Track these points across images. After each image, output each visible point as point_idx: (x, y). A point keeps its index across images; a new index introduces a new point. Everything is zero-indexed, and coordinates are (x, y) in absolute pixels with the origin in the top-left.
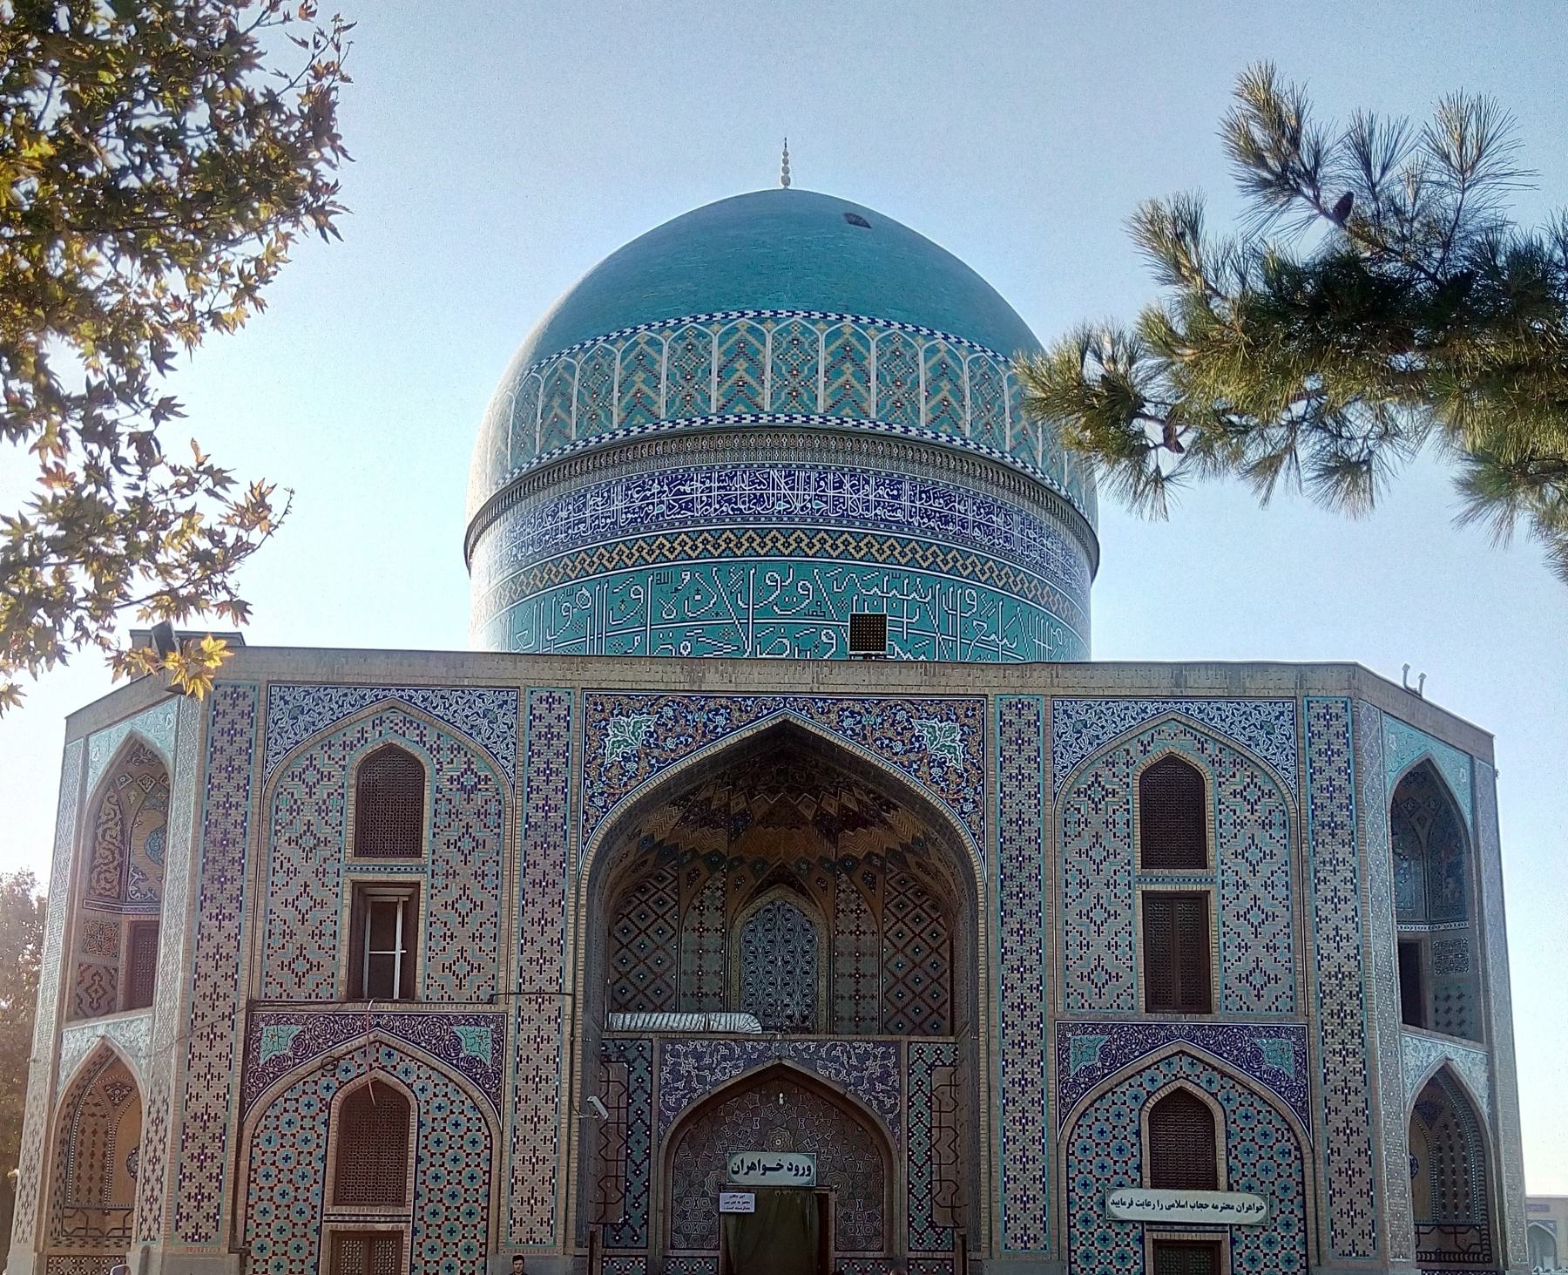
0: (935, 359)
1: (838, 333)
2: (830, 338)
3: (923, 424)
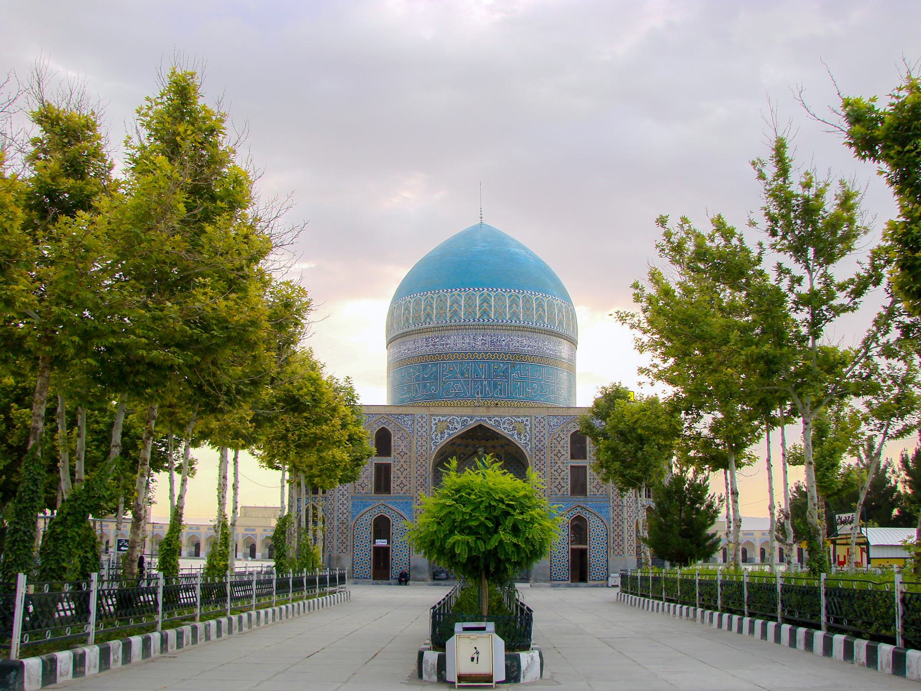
1: (483, 294)
2: (480, 296)
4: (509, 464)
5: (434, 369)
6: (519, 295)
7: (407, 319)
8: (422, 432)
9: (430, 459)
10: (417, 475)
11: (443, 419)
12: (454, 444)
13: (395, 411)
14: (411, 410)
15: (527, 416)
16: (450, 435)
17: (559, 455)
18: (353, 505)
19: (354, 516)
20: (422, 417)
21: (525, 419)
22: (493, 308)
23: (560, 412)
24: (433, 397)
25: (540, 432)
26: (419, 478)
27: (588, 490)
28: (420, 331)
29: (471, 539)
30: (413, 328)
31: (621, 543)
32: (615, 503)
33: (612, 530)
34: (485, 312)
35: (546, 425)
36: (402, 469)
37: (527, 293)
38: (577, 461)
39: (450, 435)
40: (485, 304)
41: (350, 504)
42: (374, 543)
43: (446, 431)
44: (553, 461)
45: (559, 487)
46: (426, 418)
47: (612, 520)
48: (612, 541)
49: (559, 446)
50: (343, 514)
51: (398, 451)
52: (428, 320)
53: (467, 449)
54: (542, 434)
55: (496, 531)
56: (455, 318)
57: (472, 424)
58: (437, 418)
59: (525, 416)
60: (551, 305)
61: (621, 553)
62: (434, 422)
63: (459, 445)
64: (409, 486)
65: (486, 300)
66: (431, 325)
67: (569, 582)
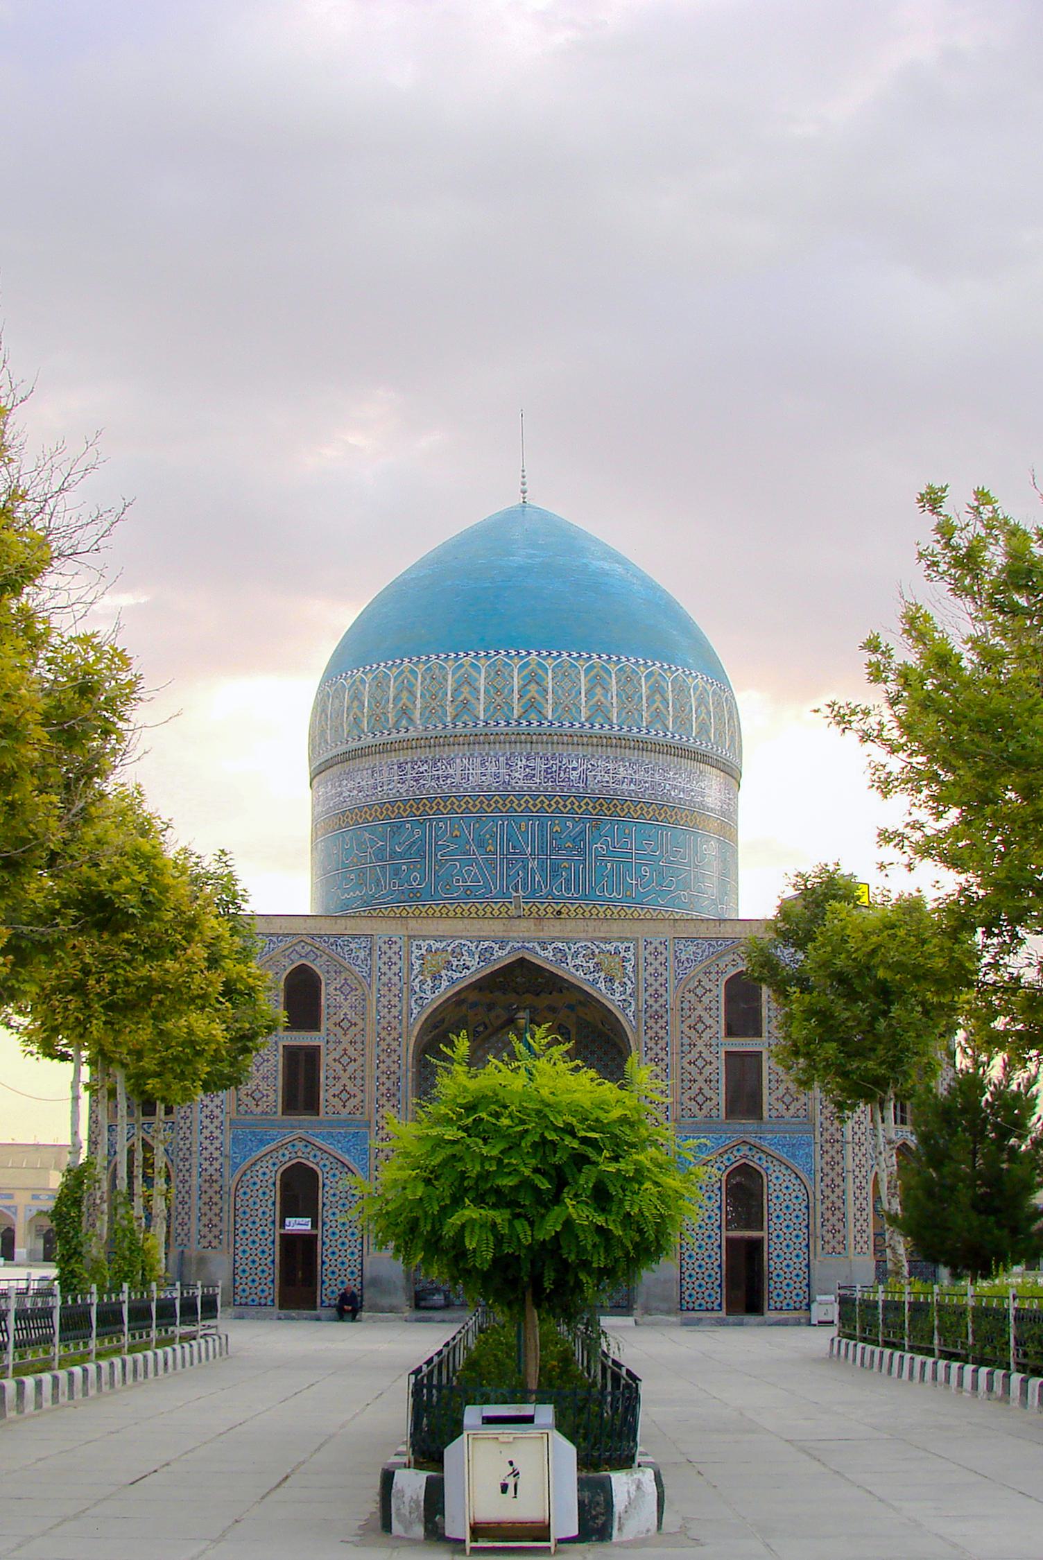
0: (592, 674)
1: (527, 665)
3: (583, 719)
4: (586, 1047)
5: (418, 833)
6: (610, 667)
7: (357, 721)
8: (390, 974)
9: (409, 1033)
10: (378, 1073)
12: (463, 1001)
13: (328, 927)
14: (365, 926)
15: (627, 939)
16: (453, 982)
17: (700, 1027)
18: (235, 1140)
19: (235, 1166)
20: (390, 942)
21: (622, 947)
22: (550, 696)
23: (703, 931)
24: (415, 896)
25: (656, 975)
26: (383, 1079)
27: (765, 1107)
28: (385, 748)
29: (499, 1216)
30: (369, 740)
31: (839, 1226)
32: (827, 1136)
33: (819, 1196)
34: (532, 706)
35: (671, 958)
36: (345, 1060)
37: (628, 662)
38: (742, 1040)
39: (453, 982)
40: (533, 687)
41: (227, 1138)
42: (283, 1225)
43: (443, 972)
44: (686, 1041)
45: (700, 1099)
46: (400, 943)
47: (819, 1175)
48: (819, 1221)
49: (699, 1007)
50: (212, 1159)
51: (336, 1019)
52: (404, 723)
53: (493, 1014)
54: (661, 980)
55: (557, 1199)
56: (465, 717)
57: (503, 957)
58: (424, 944)
59: (622, 939)
60: (680, 689)
61: (839, 1248)
62: (417, 953)
63: (474, 1005)
64: (360, 1096)
65: (534, 678)
66: (412, 734)
67: (722, 1314)
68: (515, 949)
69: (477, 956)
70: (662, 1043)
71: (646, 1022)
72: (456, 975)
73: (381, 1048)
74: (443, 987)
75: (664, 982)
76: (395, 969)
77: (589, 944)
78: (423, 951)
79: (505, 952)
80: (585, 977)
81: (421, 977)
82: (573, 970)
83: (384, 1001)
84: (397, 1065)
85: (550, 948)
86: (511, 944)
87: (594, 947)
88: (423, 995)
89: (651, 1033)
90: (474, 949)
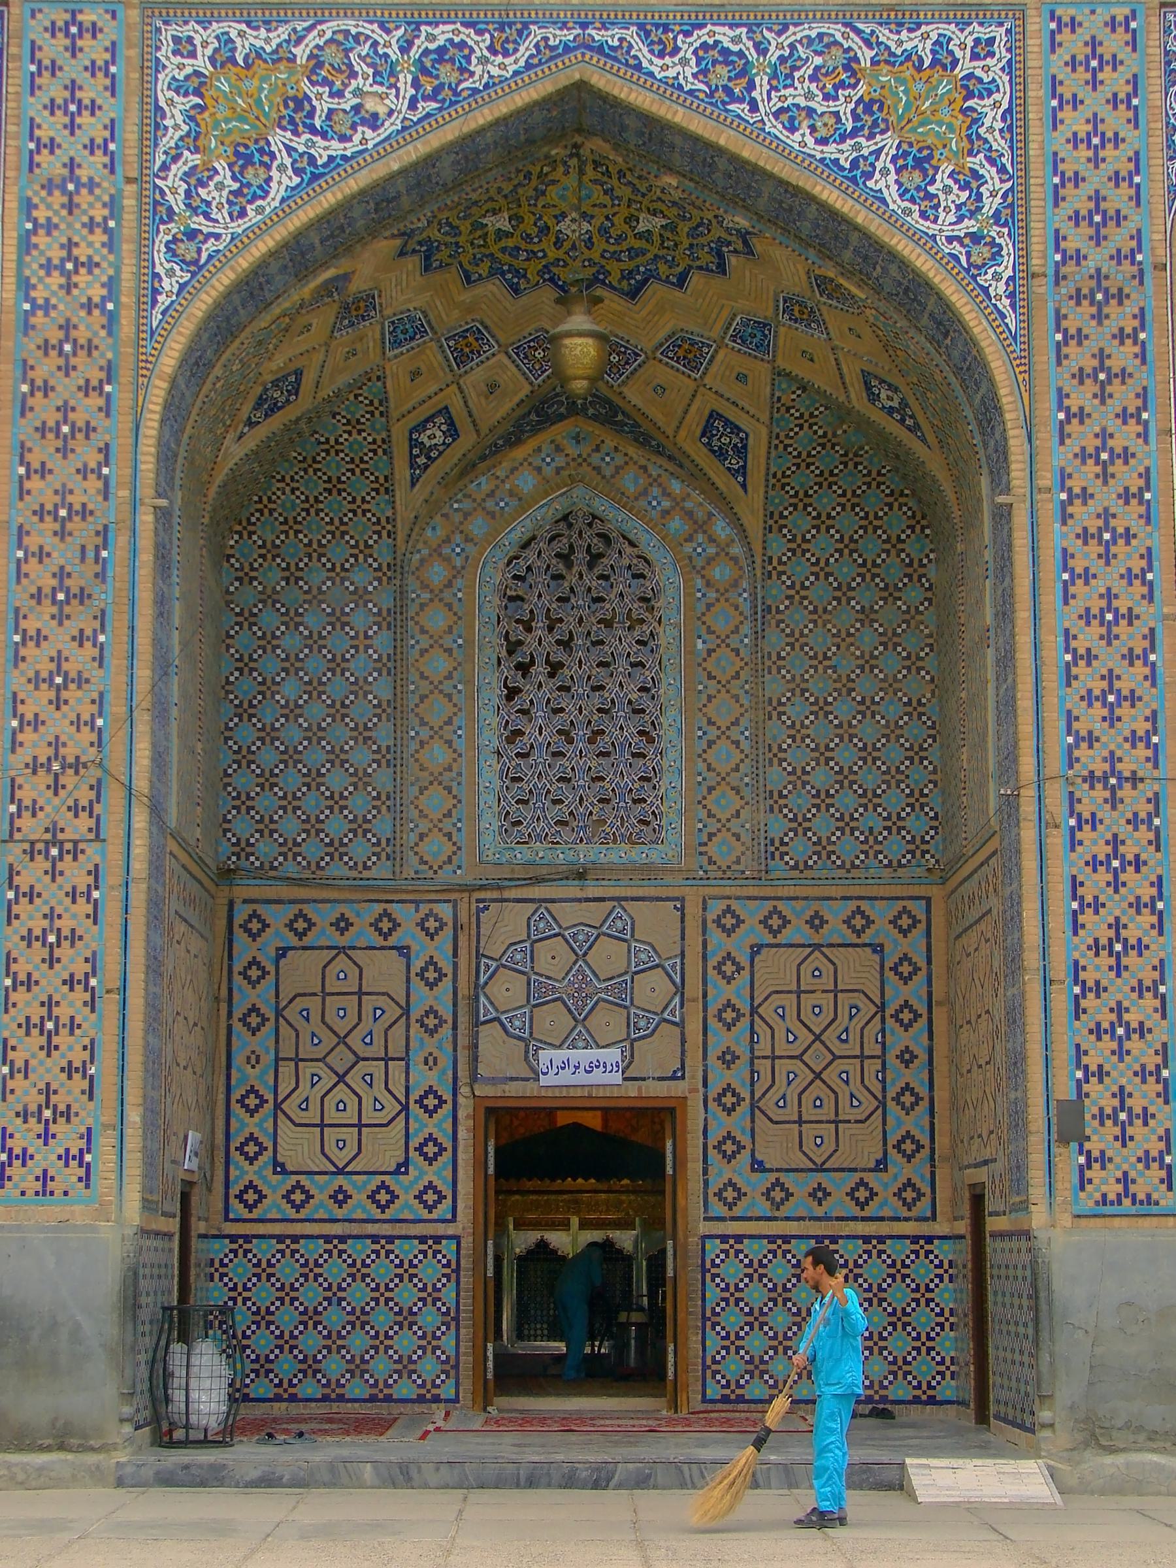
4: (803, 500)
9: (144, 367)
11: (258, 39)
43: (278, 139)
54: (1116, 159)
62: (174, 67)
68: (547, 53)
69: (405, 80)
70: (1123, 395)
71: (1059, 317)
72: (323, 150)
73: (34, 420)
74: (277, 192)
75: (1125, 167)
76: (92, 126)
77: (836, 31)
78: (202, 63)
79: (514, 64)
80: (818, 151)
81: (192, 159)
82: (775, 128)
83: (49, 247)
84: (94, 484)
85: (687, 47)
86: (535, 31)
87: (855, 42)
88: (198, 222)
89: (1080, 357)
90: (394, 53)
